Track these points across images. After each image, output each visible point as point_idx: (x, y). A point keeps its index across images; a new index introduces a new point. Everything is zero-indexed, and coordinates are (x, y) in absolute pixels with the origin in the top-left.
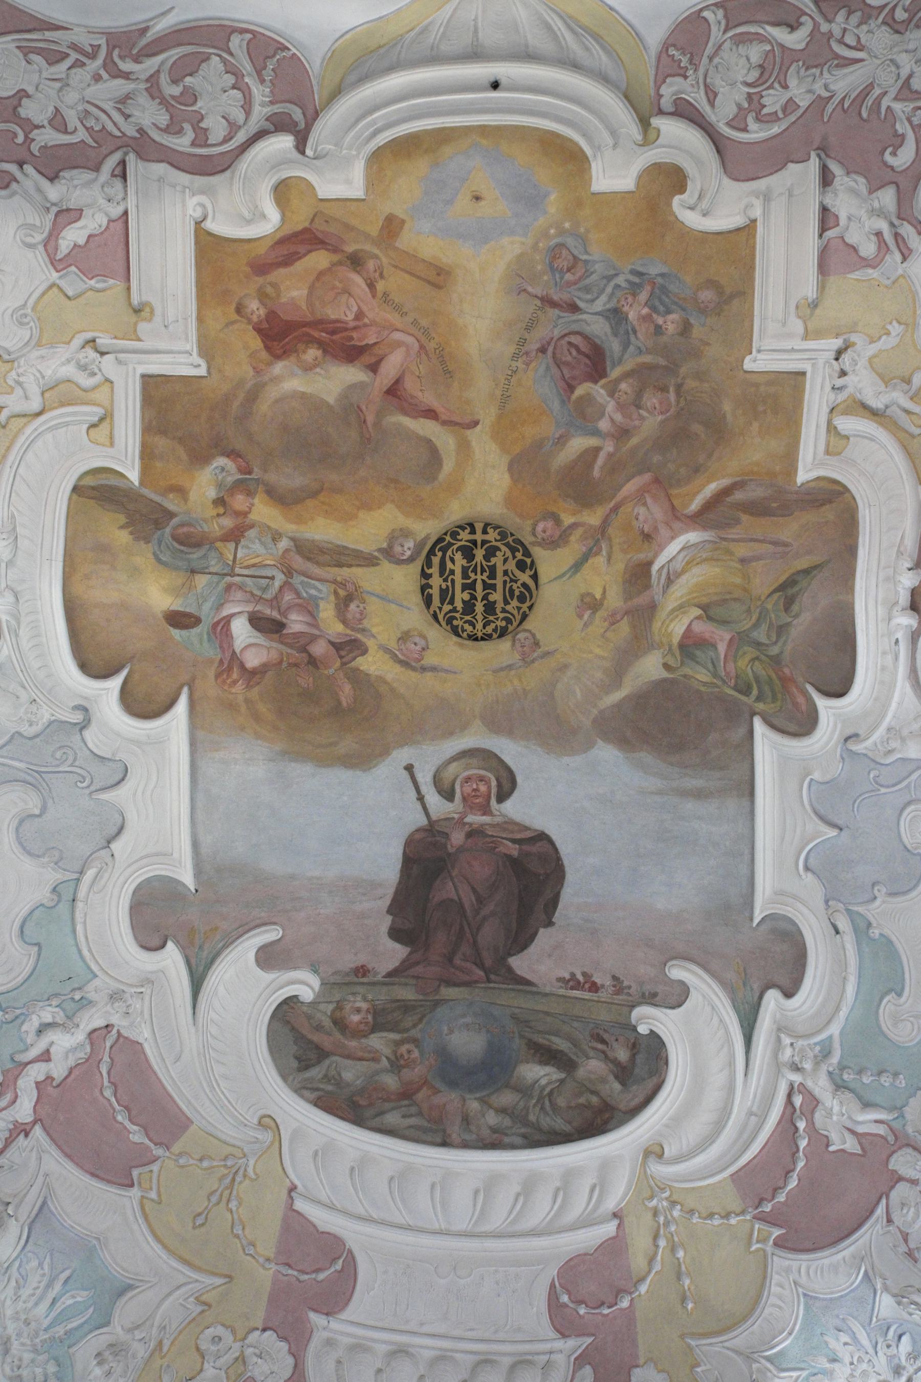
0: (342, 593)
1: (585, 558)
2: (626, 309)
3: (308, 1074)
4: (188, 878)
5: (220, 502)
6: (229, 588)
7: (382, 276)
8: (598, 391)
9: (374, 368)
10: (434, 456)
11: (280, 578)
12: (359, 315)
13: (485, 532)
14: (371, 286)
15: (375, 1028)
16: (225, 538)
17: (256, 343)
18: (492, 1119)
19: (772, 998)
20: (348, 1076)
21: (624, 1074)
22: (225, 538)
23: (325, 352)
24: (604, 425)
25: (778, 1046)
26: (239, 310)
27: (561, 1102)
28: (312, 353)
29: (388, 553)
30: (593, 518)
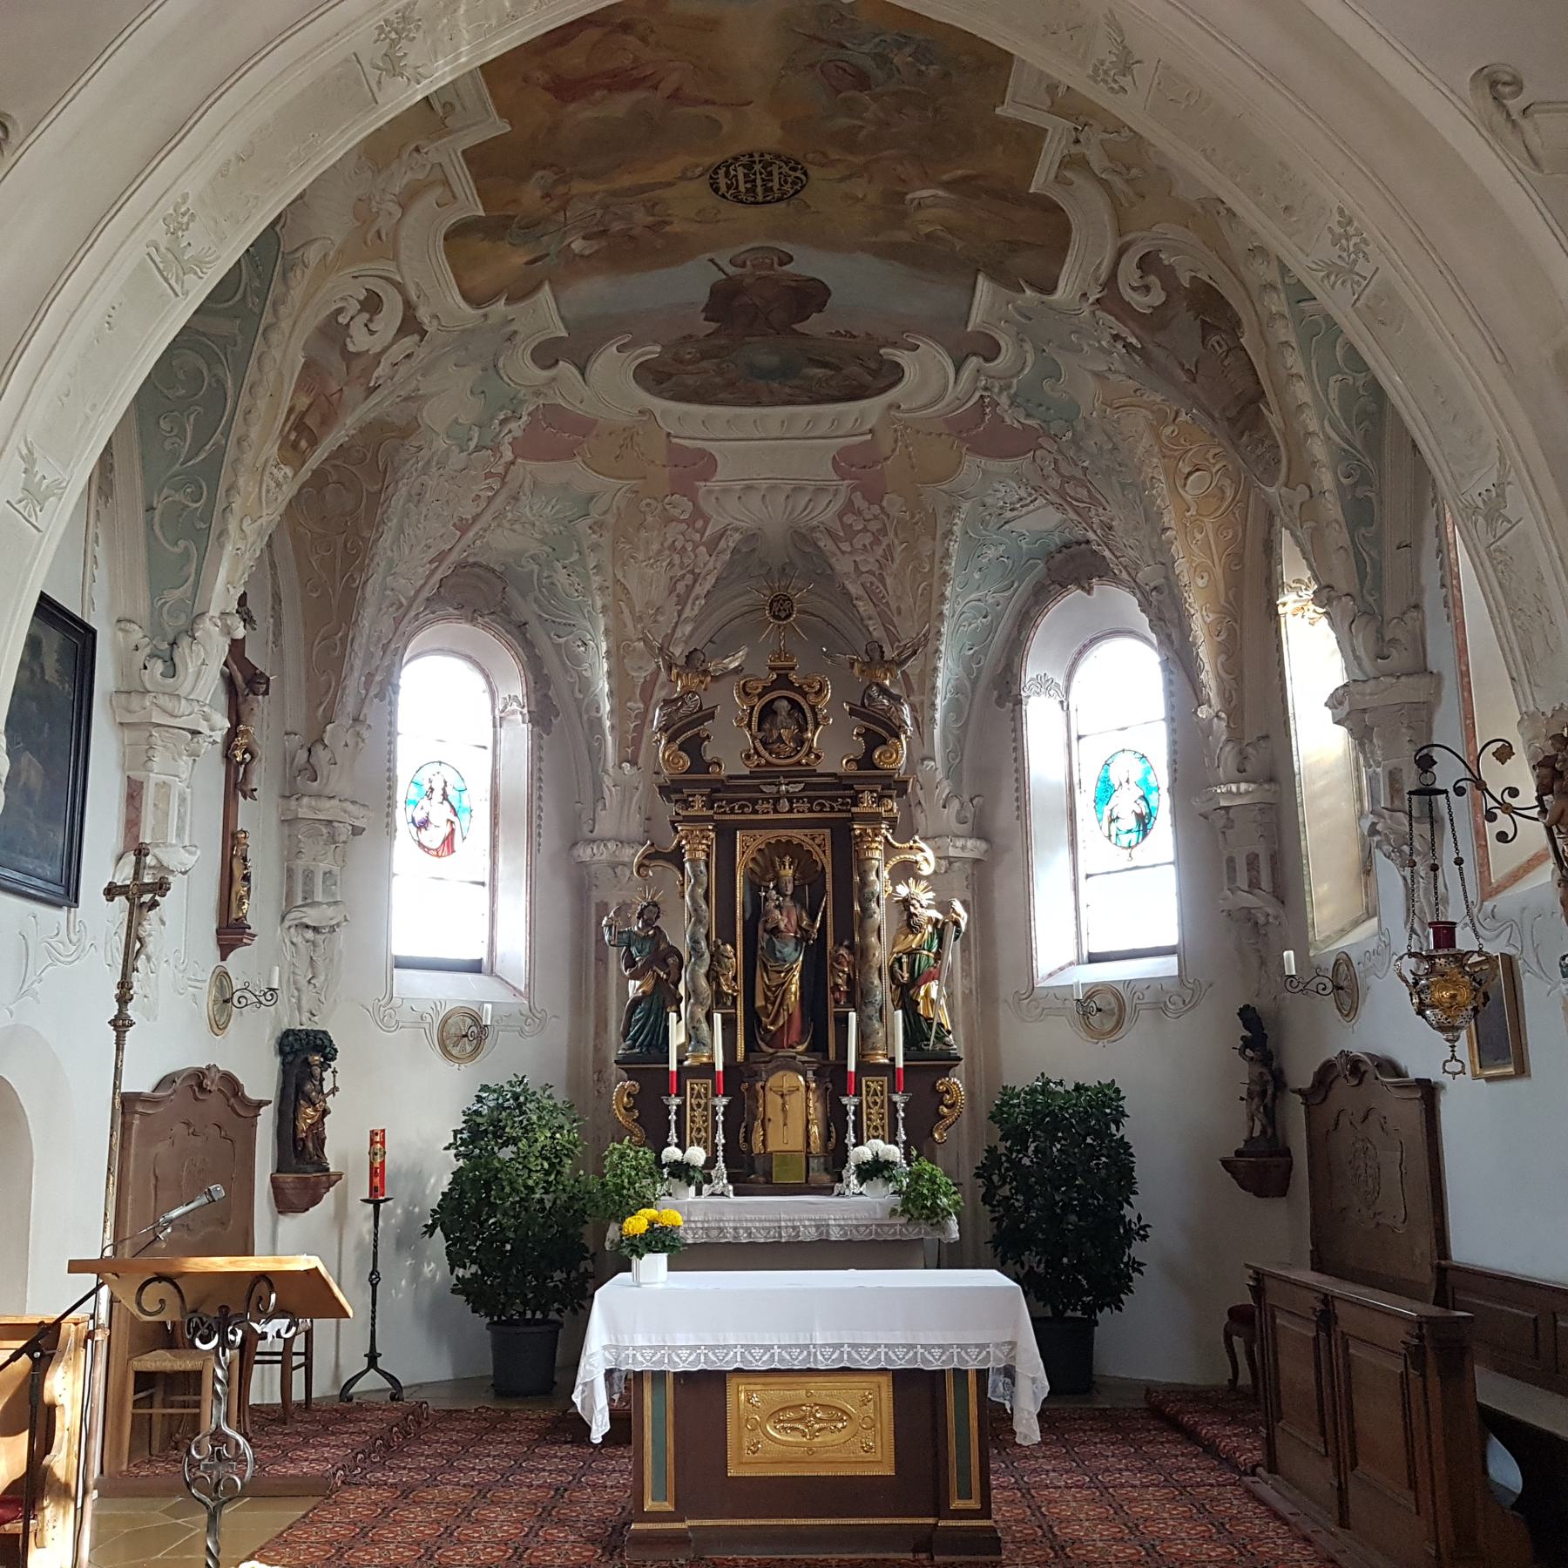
0: (648, 204)
1: (850, 176)
2: (891, 55)
3: (663, 386)
4: (565, 334)
5: (546, 195)
6: (565, 233)
7: (652, 31)
8: (865, 97)
9: (656, 88)
10: (716, 125)
11: (599, 212)
12: (636, 59)
13: (762, 155)
14: (643, 40)
15: (702, 359)
16: (556, 211)
17: (548, 97)
18: (787, 390)
19: (974, 362)
20: (690, 382)
21: (874, 373)
22: (556, 211)
23: (610, 90)
24: (867, 115)
25: (976, 380)
26: (525, 80)
27: (833, 383)
28: (598, 94)
29: (683, 177)
30: (859, 160)
